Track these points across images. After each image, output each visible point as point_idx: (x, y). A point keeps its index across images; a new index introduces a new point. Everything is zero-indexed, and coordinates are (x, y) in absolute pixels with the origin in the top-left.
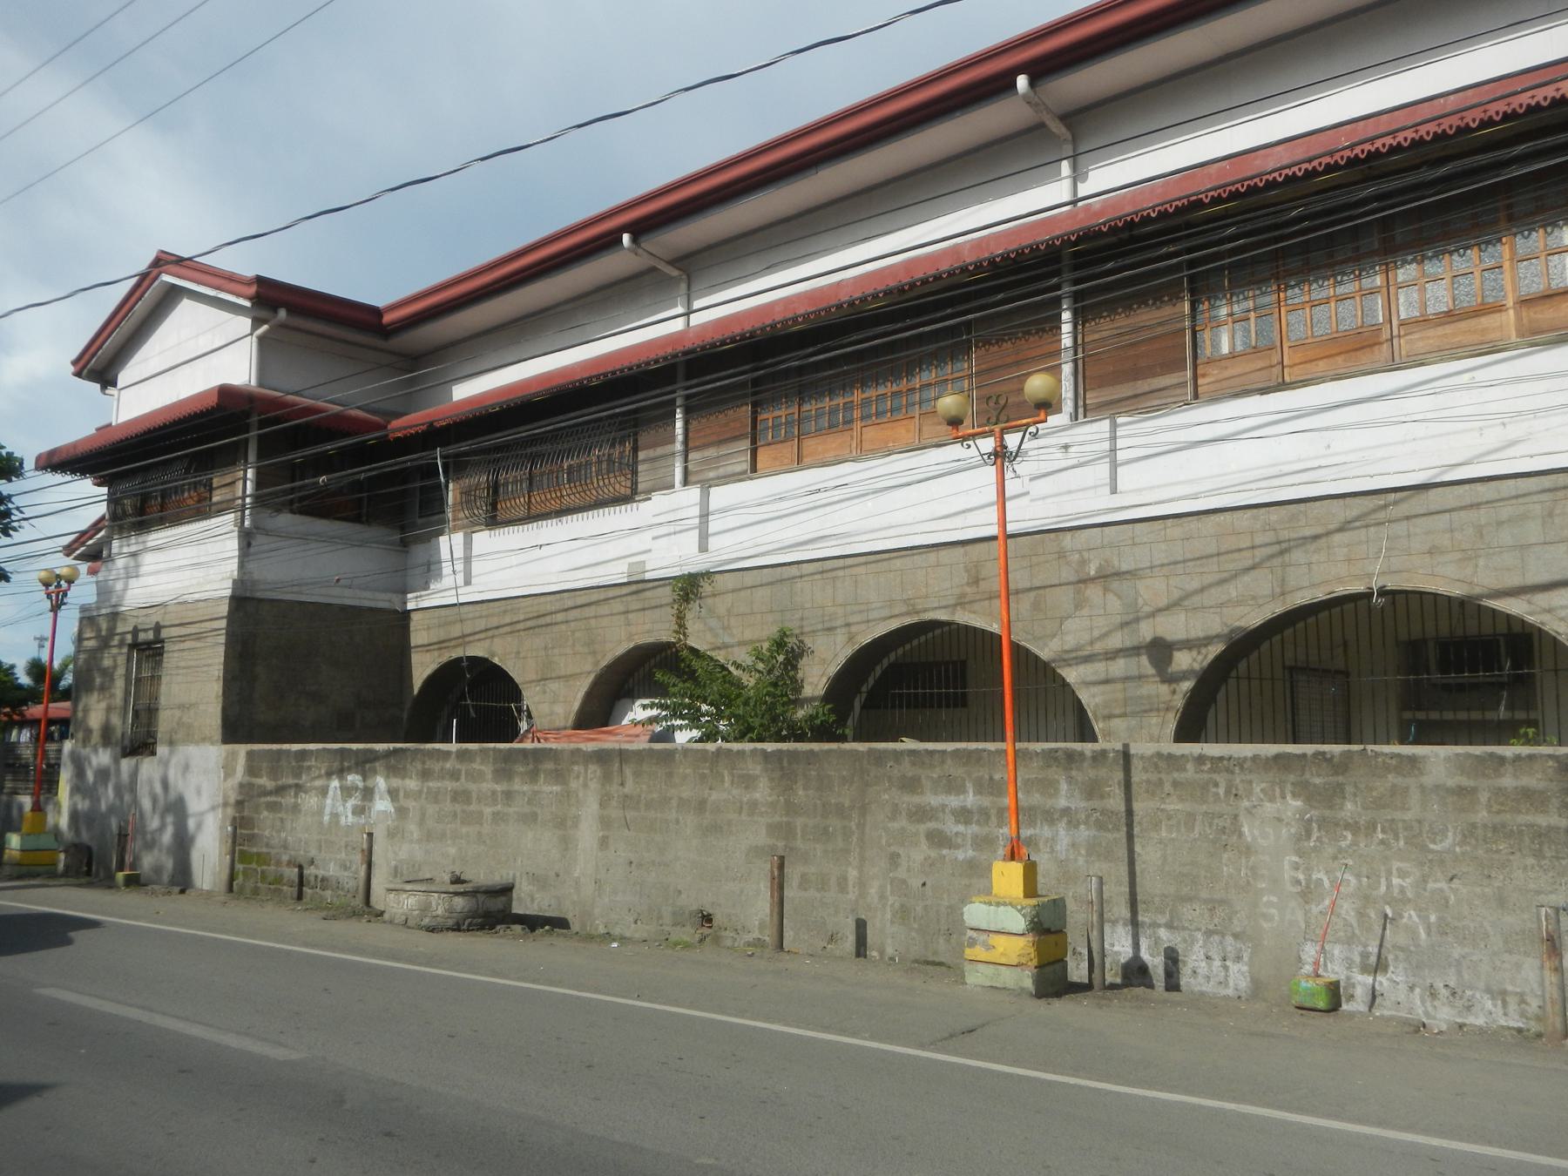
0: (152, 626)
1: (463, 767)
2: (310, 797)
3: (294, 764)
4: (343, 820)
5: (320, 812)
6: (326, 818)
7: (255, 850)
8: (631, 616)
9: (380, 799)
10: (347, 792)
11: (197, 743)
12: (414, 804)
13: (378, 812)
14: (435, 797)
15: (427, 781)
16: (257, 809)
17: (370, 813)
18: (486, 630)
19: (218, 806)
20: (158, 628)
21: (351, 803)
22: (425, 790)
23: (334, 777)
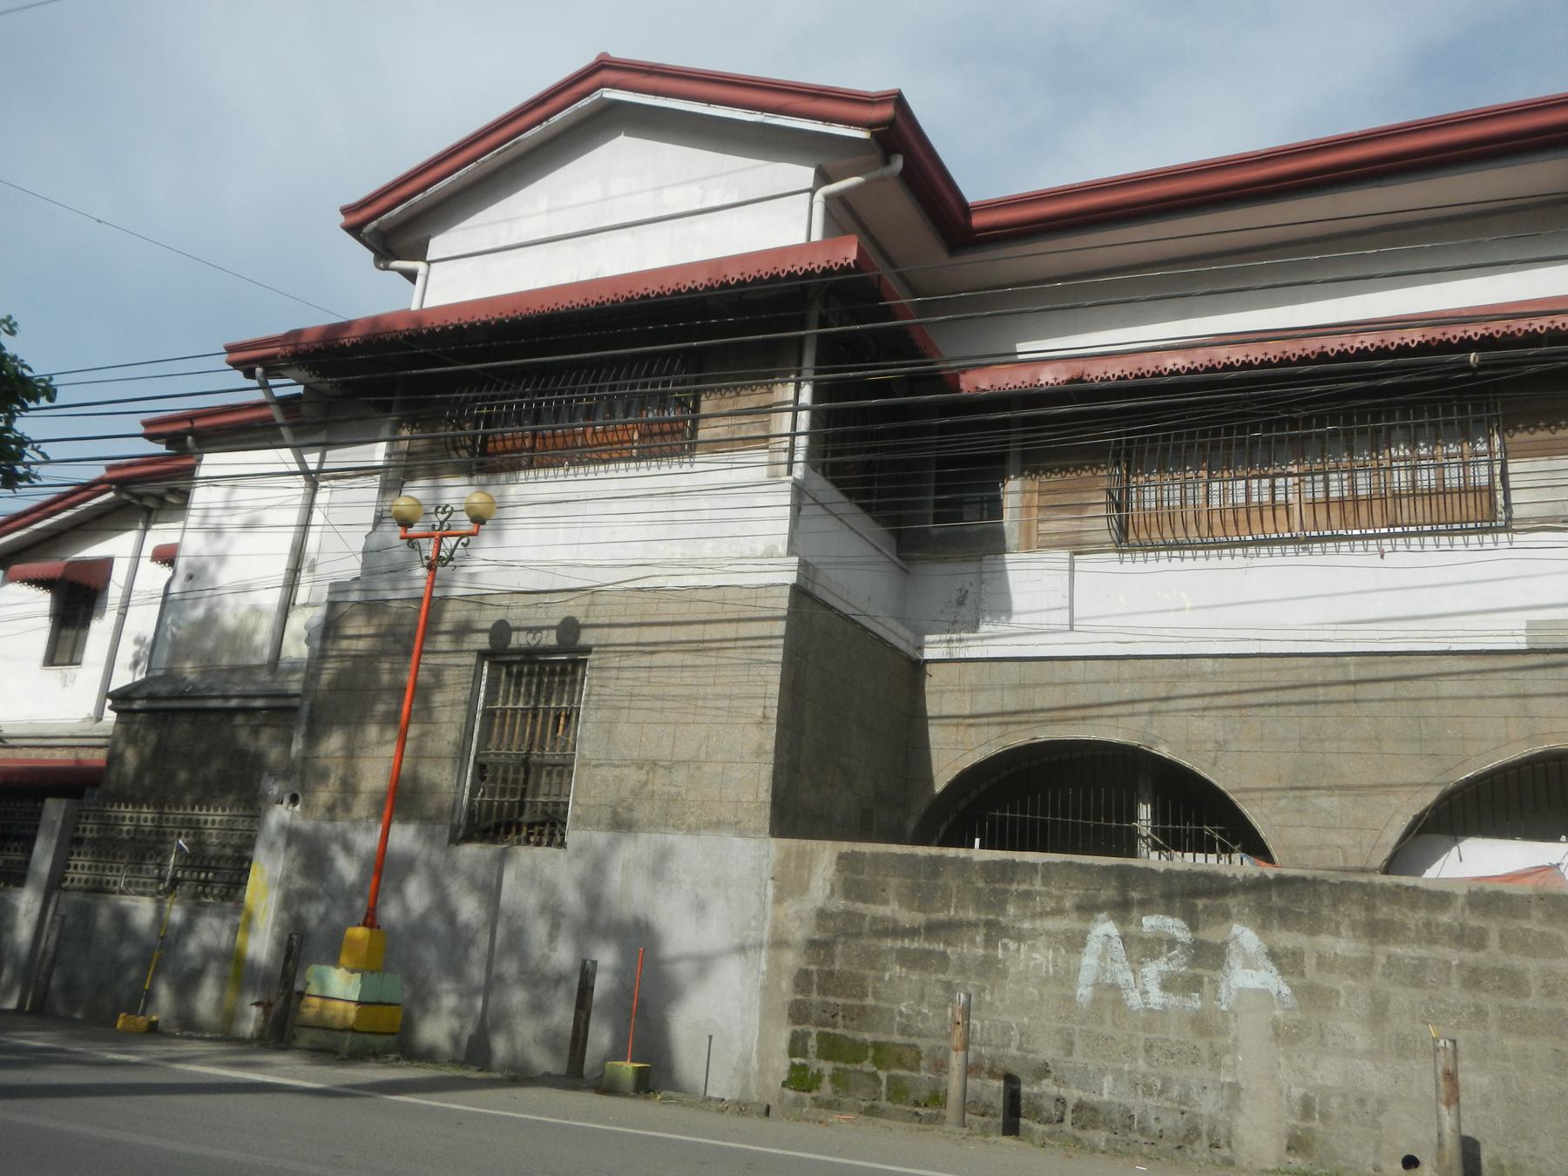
0: (556, 622)
1: (1494, 927)
2: (1033, 948)
3: (981, 884)
4: (1134, 999)
5: (1068, 978)
6: (1084, 992)
7: (868, 1037)
8: (1533, 704)
9: (1248, 964)
10: (1144, 949)
11: (690, 830)
12: (1351, 982)
13: (1240, 990)
14: (1415, 975)
15: (1385, 942)
16: (872, 958)
17: (1217, 989)
18: (1133, 702)
19: (758, 946)
20: (570, 628)
21: (1153, 971)
22: (1383, 960)
23: (1103, 916)
